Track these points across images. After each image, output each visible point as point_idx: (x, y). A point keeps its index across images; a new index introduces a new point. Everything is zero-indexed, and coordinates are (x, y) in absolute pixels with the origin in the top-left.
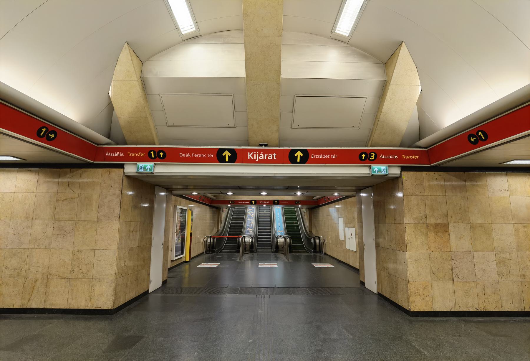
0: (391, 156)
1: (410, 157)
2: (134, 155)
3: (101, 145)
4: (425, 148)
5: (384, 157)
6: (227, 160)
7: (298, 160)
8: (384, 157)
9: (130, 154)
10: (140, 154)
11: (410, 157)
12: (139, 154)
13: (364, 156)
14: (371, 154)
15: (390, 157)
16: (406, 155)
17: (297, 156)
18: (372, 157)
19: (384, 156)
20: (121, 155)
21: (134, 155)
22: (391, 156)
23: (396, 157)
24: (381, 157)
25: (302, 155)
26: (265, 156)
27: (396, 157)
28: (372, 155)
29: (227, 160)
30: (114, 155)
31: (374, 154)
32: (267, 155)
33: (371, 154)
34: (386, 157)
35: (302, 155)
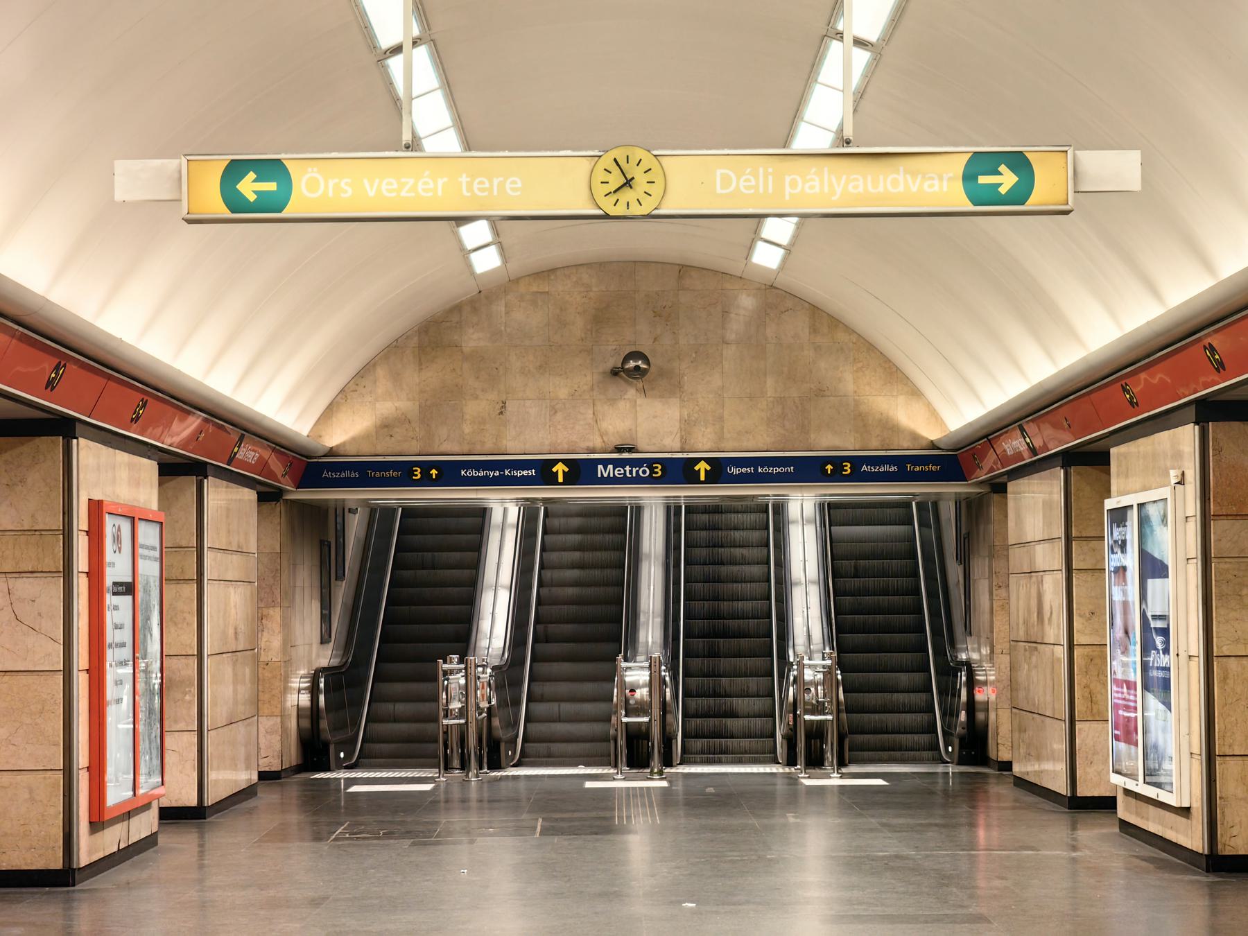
0: (884, 466)
1: (922, 468)
2: (378, 475)
3: (316, 458)
4: (948, 450)
5: (871, 469)
6: (561, 479)
7: (702, 478)
8: (871, 469)
9: (371, 473)
10: (391, 472)
11: (922, 468)
12: (390, 474)
13: (829, 467)
14: (844, 464)
15: (882, 469)
16: (914, 465)
17: (700, 469)
18: (846, 471)
19: (869, 467)
20: (353, 475)
21: (378, 475)
22: (884, 466)
23: (893, 468)
24: (864, 468)
25: (708, 468)
26: (634, 470)
27: (893, 468)
28: (846, 466)
29: (561, 479)
30: (340, 475)
31: (849, 465)
32: (637, 469)
33: (844, 464)
34: (875, 469)
35: (708, 468)
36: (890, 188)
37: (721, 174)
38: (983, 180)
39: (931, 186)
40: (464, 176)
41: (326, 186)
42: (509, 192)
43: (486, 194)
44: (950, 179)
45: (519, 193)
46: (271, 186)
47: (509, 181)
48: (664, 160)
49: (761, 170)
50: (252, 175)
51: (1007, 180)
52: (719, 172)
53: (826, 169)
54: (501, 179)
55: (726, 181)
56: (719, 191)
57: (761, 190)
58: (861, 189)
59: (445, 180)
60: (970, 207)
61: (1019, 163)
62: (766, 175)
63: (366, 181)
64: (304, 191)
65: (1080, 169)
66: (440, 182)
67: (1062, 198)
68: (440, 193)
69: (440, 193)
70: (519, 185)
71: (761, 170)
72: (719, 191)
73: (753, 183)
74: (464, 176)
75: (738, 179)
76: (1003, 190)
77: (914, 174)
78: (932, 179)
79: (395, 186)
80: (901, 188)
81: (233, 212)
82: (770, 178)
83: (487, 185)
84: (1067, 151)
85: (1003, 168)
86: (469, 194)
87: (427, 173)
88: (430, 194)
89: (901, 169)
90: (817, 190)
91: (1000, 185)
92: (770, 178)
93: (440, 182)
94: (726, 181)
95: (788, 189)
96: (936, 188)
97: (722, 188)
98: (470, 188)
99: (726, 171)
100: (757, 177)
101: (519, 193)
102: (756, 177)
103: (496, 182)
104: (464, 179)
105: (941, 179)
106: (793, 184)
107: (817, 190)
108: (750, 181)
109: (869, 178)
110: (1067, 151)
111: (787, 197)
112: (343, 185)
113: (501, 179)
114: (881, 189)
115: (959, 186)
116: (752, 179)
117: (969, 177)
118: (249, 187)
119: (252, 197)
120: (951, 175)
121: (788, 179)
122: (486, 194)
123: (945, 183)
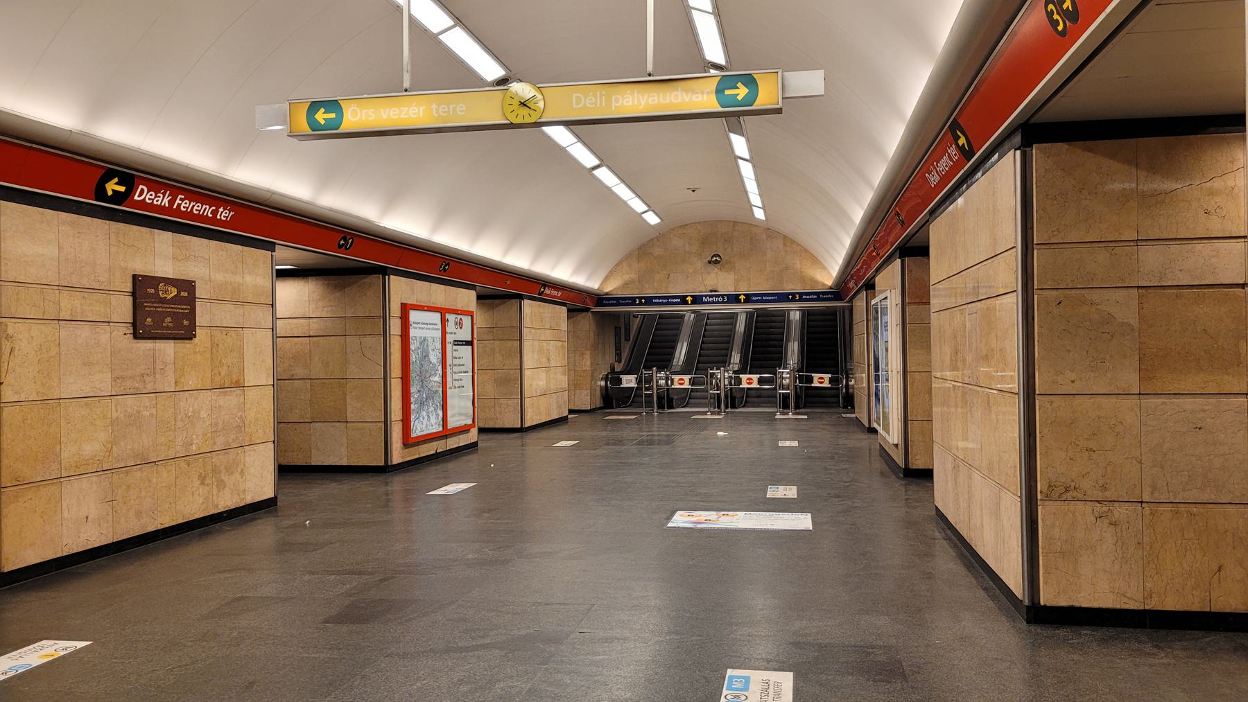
36: (673, 100)
37: (576, 97)
38: (727, 92)
39: (697, 98)
40: (434, 104)
41: (361, 114)
42: (459, 113)
43: (446, 114)
44: (708, 93)
45: (464, 113)
46: (333, 115)
47: (458, 106)
48: (543, 90)
49: (598, 93)
50: (322, 110)
51: (742, 92)
52: (575, 95)
53: (636, 91)
54: (454, 106)
55: (578, 99)
56: (574, 106)
57: (598, 105)
58: (656, 102)
59: (424, 107)
60: (721, 109)
61: (750, 81)
62: (601, 95)
63: (382, 110)
64: (350, 118)
65: (786, 83)
66: (421, 108)
67: (775, 101)
68: (421, 115)
69: (421, 115)
70: (464, 109)
71: (598, 93)
72: (574, 106)
73: (594, 101)
74: (434, 104)
75: (585, 98)
76: (739, 98)
77: (687, 91)
78: (697, 93)
79: (397, 112)
80: (679, 100)
81: (313, 131)
82: (604, 97)
83: (447, 109)
84: (777, 72)
85: (739, 85)
86: (436, 115)
87: (414, 104)
88: (416, 116)
89: (680, 88)
90: (631, 103)
91: (738, 94)
92: (604, 97)
93: (421, 108)
94: (578, 99)
95: (613, 103)
96: (700, 99)
97: (576, 105)
98: (437, 112)
99: (578, 95)
100: (596, 97)
101: (464, 113)
102: (596, 97)
103: (451, 107)
104: (434, 106)
105: (703, 93)
106: (617, 100)
107: (631, 103)
108: (592, 99)
109: (661, 95)
110: (777, 72)
111: (613, 108)
112: (370, 113)
113: (454, 106)
114: (668, 101)
115: (714, 96)
116: (593, 99)
117: (719, 91)
118: (321, 116)
119: (323, 122)
120: (709, 90)
121: (613, 98)
122: (446, 114)
123: (705, 96)
